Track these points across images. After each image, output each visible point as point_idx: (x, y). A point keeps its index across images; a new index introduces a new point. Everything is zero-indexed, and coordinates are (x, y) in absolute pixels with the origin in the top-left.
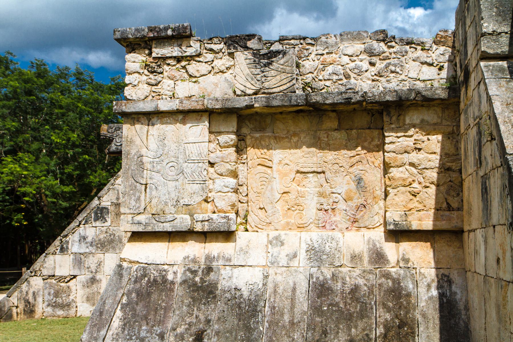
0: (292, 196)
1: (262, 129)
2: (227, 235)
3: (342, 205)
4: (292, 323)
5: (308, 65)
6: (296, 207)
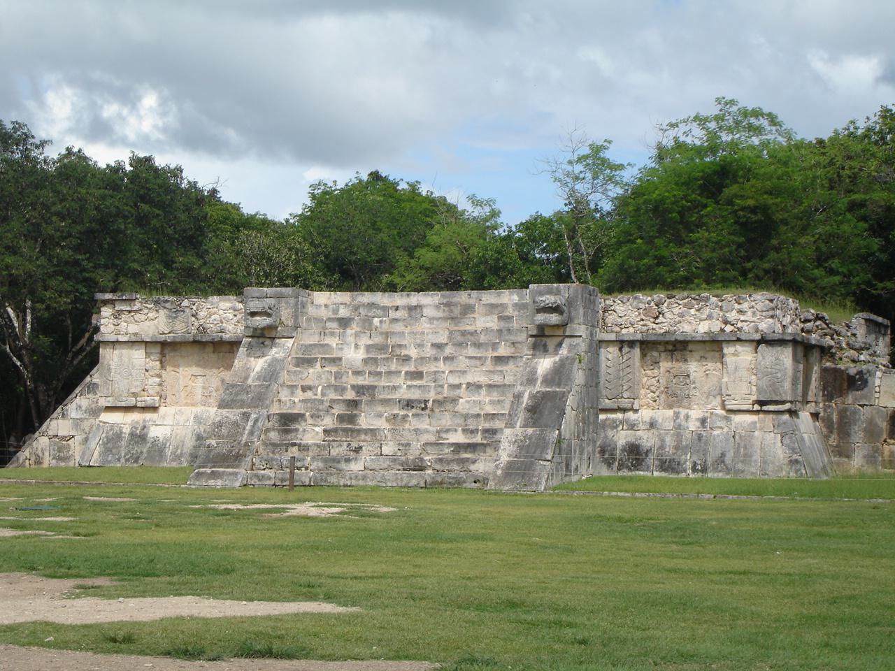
0: (189, 388)
1: (175, 350)
2: (154, 409)
3: (214, 394)
4: (181, 453)
5: (202, 314)
6: (191, 394)
